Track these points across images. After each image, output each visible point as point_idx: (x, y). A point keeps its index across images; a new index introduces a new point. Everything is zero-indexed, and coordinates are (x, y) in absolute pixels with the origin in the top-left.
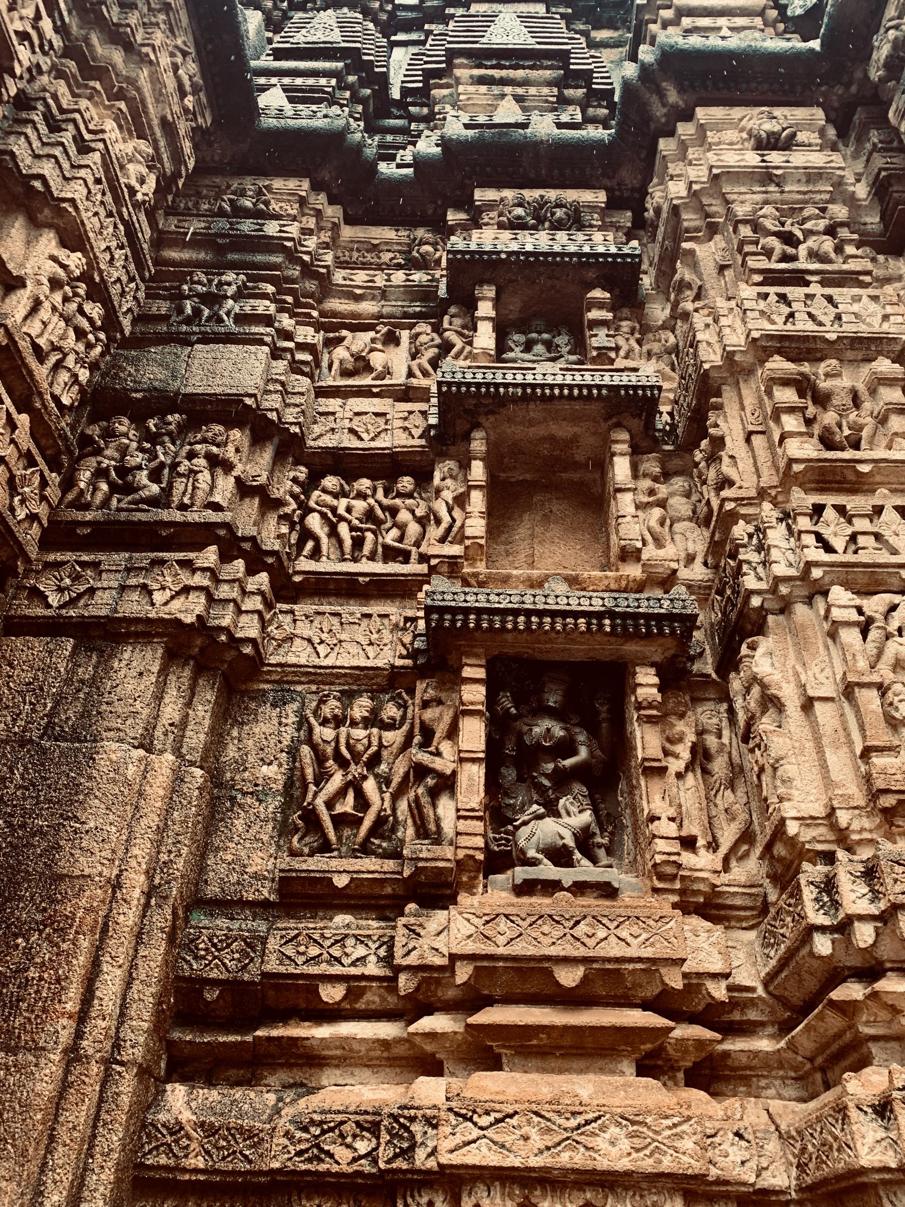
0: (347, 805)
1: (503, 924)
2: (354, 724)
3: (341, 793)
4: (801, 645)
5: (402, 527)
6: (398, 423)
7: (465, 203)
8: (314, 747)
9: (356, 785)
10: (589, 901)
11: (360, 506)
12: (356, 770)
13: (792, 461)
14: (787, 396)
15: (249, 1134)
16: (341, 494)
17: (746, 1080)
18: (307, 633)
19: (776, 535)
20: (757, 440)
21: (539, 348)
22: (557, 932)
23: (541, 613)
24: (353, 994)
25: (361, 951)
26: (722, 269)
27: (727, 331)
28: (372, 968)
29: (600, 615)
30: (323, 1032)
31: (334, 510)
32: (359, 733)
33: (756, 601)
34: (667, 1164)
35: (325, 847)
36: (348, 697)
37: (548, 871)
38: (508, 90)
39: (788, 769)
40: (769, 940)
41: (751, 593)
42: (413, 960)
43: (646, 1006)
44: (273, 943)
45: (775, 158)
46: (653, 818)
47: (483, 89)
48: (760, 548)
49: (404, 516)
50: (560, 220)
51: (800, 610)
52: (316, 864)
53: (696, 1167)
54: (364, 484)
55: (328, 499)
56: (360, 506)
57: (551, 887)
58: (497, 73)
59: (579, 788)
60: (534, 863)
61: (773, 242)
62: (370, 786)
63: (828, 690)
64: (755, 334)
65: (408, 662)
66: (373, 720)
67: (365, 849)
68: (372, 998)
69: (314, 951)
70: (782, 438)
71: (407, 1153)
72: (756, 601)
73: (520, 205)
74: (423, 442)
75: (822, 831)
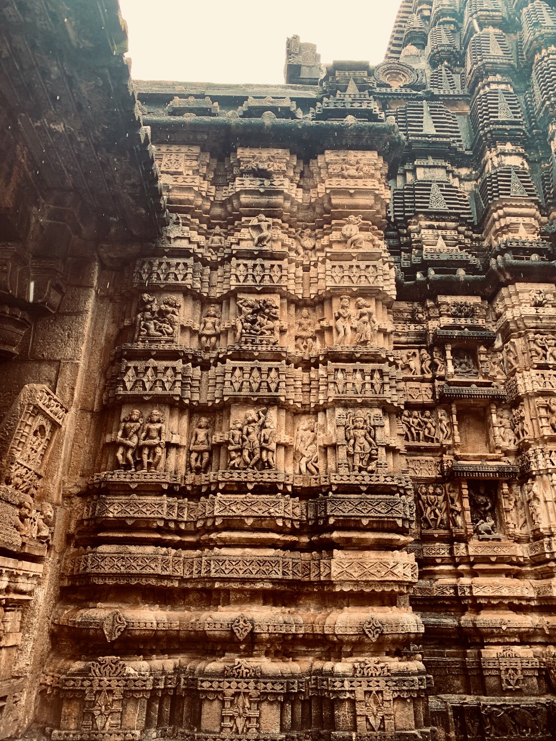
0: (433, 517)
1: (479, 549)
2: (430, 494)
3: (431, 513)
4: (545, 486)
5: (429, 429)
6: (424, 393)
7: (434, 299)
8: (422, 501)
9: (434, 511)
10: (495, 542)
11: (416, 421)
12: (433, 507)
13: (544, 436)
14: (543, 412)
15: (429, 589)
16: (410, 416)
17: (524, 575)
18: (412, 466)
19: (540, 457)
20: (534, 421)
21: (464, 365)
22: (490, 550)
23: (481, 472)
24: (443, 560)
25: (443, 552)
26: (524, 353)
27: (527, 385)
28: (447, 555)
29: (495, 472)
30: (437, 568)
31: (409, 422)
32: (432, 497)
33: (534, 473)
34: (515, 595)
35: (429, 527)
36: (427, 486)
37: (486, 536)
38: (440, 232)
39: (541, 516)
40: (532, 549)
41: (533, 471)
42: (458, 555)
43: (507, 563)
44: (424, 550)
45: (541, 310)
46: (508, 523)
47: (431, 231)
48: (535, 458)
49: (429, 425)
50: (467, 313)
51: (545, 476)
52: (429, 532)
53: (521, 595)
54: (415, 413)
55: (406, 419)
56: (416, 421)
57: (488, 540)
58: (436, 224)
59: (490, 514)
60: (483, 534)
61: (539, 350)
62: (437, 511)
63: (550, 499)
64: (536, 391)
65: (440, 476)
66: (434, 493)
67: (440, 528)
68: (446, 561)
69: (433, 552)
70: (542, 427)
71: (464, 593)
72: (534, 473)
73: (454, 306)
74: (432, 400)
75: (547, 531)
